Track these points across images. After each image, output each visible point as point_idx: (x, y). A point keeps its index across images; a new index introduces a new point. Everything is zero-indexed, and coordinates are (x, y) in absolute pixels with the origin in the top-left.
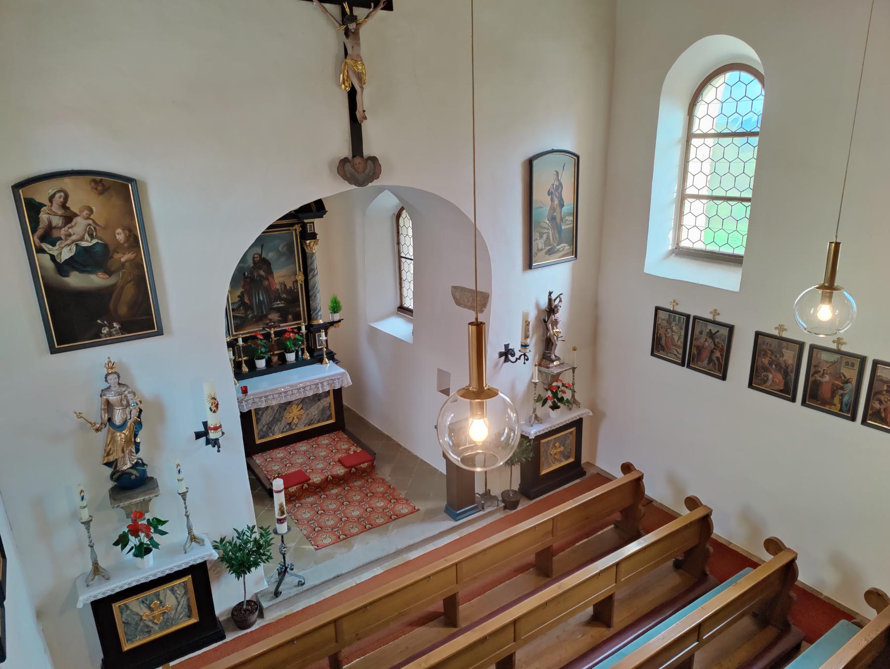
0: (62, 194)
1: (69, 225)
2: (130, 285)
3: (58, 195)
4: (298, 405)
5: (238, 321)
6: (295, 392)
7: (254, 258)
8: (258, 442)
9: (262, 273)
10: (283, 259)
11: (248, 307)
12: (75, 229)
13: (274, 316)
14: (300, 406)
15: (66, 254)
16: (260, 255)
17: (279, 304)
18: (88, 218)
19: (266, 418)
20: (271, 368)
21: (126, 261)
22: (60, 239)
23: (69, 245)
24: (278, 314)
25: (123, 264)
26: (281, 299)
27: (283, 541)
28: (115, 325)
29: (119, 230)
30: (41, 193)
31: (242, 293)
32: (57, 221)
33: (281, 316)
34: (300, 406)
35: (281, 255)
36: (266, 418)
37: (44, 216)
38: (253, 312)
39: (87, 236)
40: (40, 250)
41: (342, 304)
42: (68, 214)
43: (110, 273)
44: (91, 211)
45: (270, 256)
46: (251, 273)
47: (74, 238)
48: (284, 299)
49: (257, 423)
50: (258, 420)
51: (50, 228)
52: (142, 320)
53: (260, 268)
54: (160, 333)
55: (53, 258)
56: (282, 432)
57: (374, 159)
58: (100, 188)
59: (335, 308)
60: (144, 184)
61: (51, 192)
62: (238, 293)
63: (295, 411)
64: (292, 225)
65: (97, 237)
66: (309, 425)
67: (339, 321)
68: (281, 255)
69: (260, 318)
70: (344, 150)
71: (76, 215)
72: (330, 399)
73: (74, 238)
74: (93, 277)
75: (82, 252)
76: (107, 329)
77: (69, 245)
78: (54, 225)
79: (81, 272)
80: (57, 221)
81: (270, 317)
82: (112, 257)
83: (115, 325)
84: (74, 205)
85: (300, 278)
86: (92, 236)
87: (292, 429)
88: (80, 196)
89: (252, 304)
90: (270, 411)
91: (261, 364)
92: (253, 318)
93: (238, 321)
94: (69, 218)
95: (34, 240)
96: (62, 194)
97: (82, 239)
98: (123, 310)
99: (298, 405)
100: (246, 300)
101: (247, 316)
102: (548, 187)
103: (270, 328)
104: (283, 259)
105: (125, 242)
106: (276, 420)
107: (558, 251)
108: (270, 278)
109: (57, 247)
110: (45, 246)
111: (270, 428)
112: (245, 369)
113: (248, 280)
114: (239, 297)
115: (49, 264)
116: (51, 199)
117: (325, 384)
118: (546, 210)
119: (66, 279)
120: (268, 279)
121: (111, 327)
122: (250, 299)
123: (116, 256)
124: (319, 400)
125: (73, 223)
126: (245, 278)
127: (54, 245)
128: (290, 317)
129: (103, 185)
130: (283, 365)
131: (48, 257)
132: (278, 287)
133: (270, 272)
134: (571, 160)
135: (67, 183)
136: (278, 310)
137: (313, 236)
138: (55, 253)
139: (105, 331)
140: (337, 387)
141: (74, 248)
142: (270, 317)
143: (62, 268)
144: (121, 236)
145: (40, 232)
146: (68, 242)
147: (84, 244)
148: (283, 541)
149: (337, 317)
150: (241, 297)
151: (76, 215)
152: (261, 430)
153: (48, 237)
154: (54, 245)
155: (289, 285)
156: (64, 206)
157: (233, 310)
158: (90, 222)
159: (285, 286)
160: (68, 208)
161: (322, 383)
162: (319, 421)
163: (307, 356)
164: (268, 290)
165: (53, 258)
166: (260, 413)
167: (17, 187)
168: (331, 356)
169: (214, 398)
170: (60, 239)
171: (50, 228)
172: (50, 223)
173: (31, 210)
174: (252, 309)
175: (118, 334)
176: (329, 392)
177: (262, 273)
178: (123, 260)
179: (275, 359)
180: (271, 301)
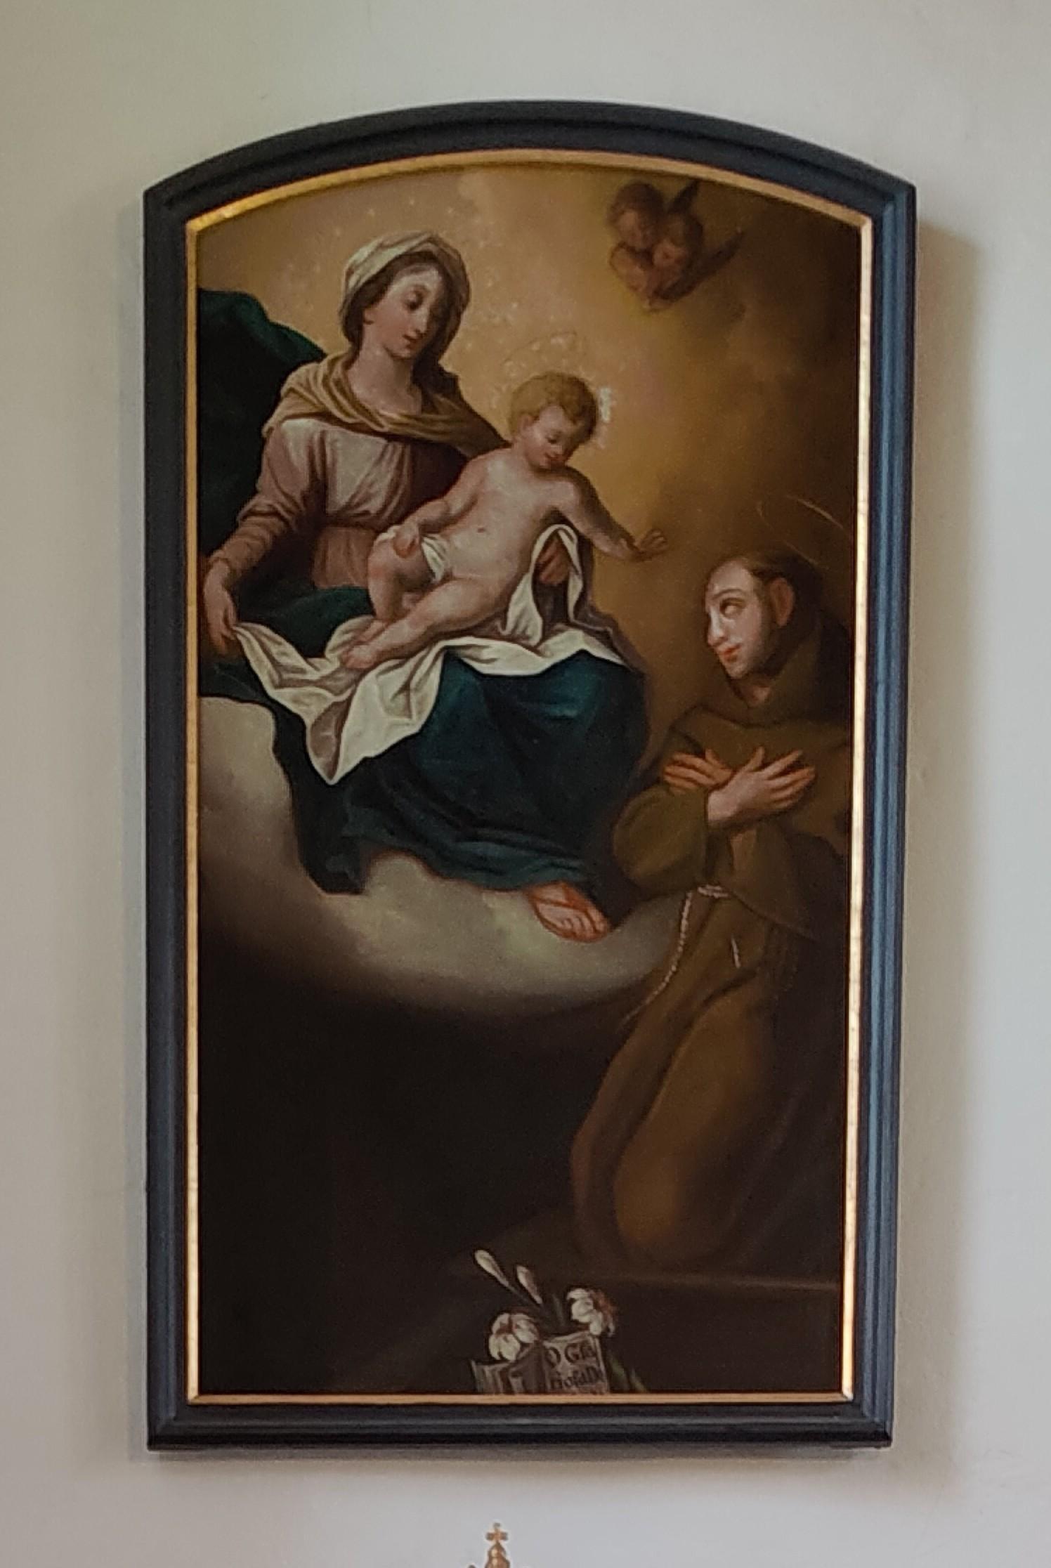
0: (430, 279)
1: (431, 511)
2: (727, 1008)
3: (402, 286)
12: (460, 539)
15: (377, 718)
18: (556, 469)
21: (735, 824)
22: (360, 604)
23: (401, 655)
25: (716, 840)
28: (581, 1305)
29: (737, 579)
30: (305, 275)
32: (363, 470)
37: (291, 430)
39: (523, 602)
40: (231, 678)
42: (439, 427)
43: (616, 896)
44: (584, 412)
47: (443, 603)
51: (316, 516)
55: (289, 729)
58: (669, 251)
61: (368, 258)
65: (585, 617)
71: (486, 439)
73: (443, 603)
75: (481, 713)
76: (525, 1332)
77: (401, 655)
78: (341, 496)
79: (443, 864)
80: (363, 470)
82: (653, 779)
83: (581, 1305)
84: (486, 372)
86: (555, 611)
88: (544, 305)
94: (438, 456)
95: (211, 589)
96: (430, 279)
97: (489, 621)
98: (652, 1199)
105: (765, 667)
109: (329, 664)
110: (266, 651)
115: (260, 780)
116: (354, 322)
119: (338, 903)
121: (552, 1319)
123: (687, 772)
125: (457, 498)
127: (312, 649)
129: (696, 230)
131: (257, 726)
135: (476, 203)
138: (309, 706)
139: (510, 1340)
141: (429, 675)
143: (342, 820)
144: (736, 630)
145: (239, 549)
146: (404, 631)
147: (500, 658)
151: (486, 439)
153: (295, 590)
154: (312, 649)
156: (425, 370)
158: (564, 495)
160: (449, 384)
165: (290, 736)
167: (172, 202)
170: (360, 604)
171: (316, 516)
172: (320, 484)
173: (215, 367)
175: (584, 1380)
178: (720, 806)
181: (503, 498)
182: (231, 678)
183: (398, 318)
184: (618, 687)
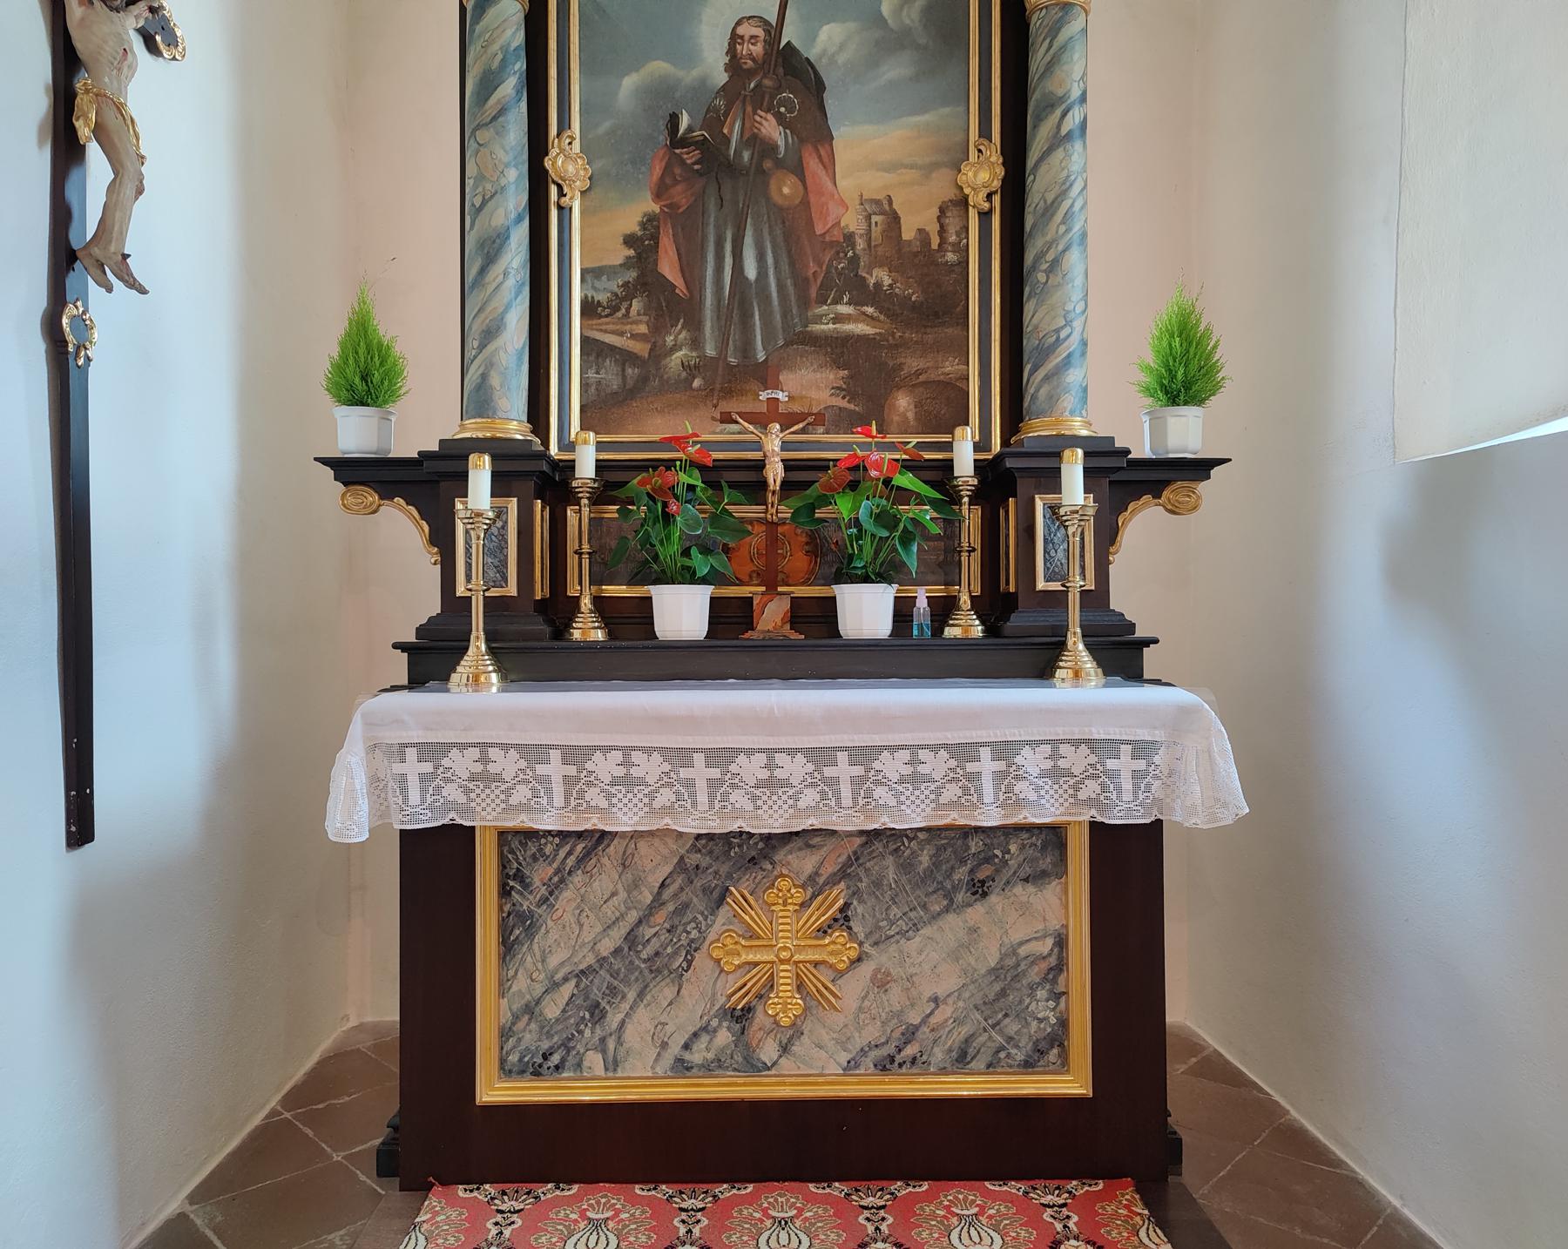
4: (815, 886)
5: (610, 375)
6: (794, 769)
7: (735, 38)
8: (492, 1090)
9: (770, 128)
10: (896, 69)
13: (810, 384)
14: (838, 895)
16: (773, 32)
17: (850, 320)
20: (731, 647)
24: (833, 376)
26: (862, 294)
31: (650, 222)
33: (849, 392)
34: (838, 895)
38: (696, 343)
41: (1233, 357)
45: (826, 41)
46: (714, 120)
48: (874, 296)
49: (507, 947)
50: (517, 930)
53: (761, 100)
56: (682, 1067)
59: (1184, 378)
62: (630, 221)
63: (775, 928)
66: (885, 1066)
67: (1200, 468)
68: (889, 41)
69: (732, 379)
72: (1064, 908)
85: (983, 175)
87: (753, 1066)
90: (604, 880)
91: (682, 612)
92: (691, 370)
93: (610, 375)
99: (815, 886)
100: (668, 267)
101: (659, 354)
103: (761, 421)
104: (896, 69)
106: (646, 960)
108: (812, 164)
111: (597, 1013)
112: (588, 629)
113: (691, 156)
114: (629, 241)
117: (1032, 761)
120: (799, 171)
122: (690, 265)
124: (980, 890)
126: (677, 141)
128: (903, 403)
130: (816, 647)
132: (852, 221)
133: (814, 130)
136: (839, 350)
140: (1125, 811)
149: (1186, 433)
150: (643, 245)
152: (531, 1010)
155: (917, 220)
157: (589, 308)
159: (894, 220)
161: (1005, 750)
162: (962, 1059)
163: (967, 626)
164: (793, 229)
166: (540, 874)
168: (1122, 653)
174: (694, 324)
176: (1055, 835)
177: (770, 128)
179: (772, 616)
180: (805, 294)
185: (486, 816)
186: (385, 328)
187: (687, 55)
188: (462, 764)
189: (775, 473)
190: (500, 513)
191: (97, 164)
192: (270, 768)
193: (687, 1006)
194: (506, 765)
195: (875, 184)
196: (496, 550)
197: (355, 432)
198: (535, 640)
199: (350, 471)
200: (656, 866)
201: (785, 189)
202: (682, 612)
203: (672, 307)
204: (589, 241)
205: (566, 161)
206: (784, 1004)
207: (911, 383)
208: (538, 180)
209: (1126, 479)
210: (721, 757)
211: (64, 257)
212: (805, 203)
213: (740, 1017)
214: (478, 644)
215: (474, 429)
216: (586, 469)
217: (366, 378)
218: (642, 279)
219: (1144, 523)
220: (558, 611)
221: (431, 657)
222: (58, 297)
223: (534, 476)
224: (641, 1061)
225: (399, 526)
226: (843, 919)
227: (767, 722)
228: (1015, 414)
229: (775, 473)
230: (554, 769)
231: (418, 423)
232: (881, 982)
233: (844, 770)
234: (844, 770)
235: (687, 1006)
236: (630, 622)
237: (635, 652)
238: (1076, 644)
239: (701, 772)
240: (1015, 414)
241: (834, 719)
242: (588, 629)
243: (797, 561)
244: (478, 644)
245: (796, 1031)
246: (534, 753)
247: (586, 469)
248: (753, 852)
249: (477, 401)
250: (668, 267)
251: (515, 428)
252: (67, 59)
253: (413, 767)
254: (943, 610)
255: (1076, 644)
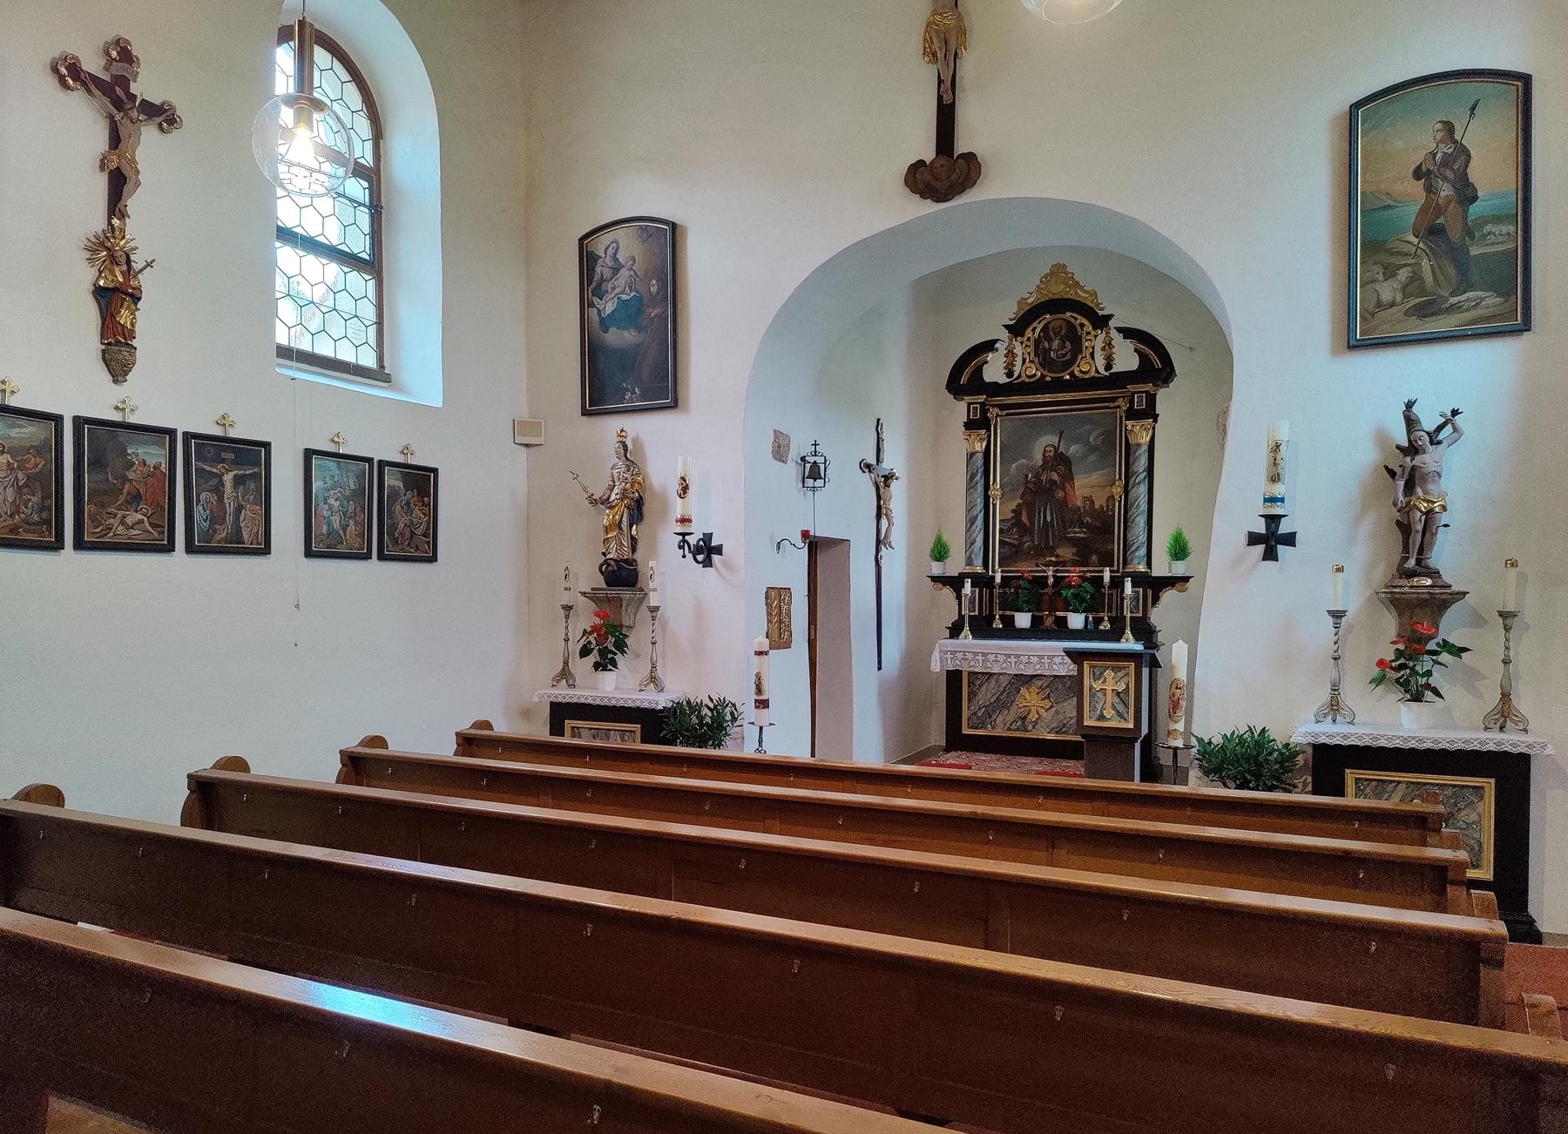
8: (966, 731)
11: (1024, 530)
13: (1066, 552)
14: (1047, 691)
15: (609, 307)
16: (1056, 449)
17: (1078, 533)
19: (986, 695)
20: (1037, 631)
26: (1082, 525)
27: (760, 742)
30: (601, 245)
32: (607, 273)
33: (1077, 554)
34: (1047, 691)
35: (1093, 449)
36: (986, 695)
37: (598, 269)
41: (1192, 545)
43: (639, 329)
45: (1073, 450)
46: (1037, 476)
48: (1087, 526)
51: (602, 280)
52: (662, 388)
54: (674, 405)
57: (970, 158)
59: (1179, 551)
60: (684, 228)
62: (1013, 505)
63: (1030, 698)
64: (1114, 399)
67: (1186, 579)
70: (929, 154)
74: (626, 334)
75: (623, 304)
80: (607, 273)
81: (1059, 551)
84: (621, 257)
85: (1118, 490)
87: (1026, 730)
88: (627, 245)
89: (1032, 524)
91: (1023, 620)
94: (616, 270)
100: (1024, 519)
101: (1020, 545)
102: (1418, 158)
104: (1092, 458)
107: (1453, 309)
110: (596, 300)
112: (998, 624)
118: (1410, 213)
122: (1031, 517)
132: (1079, 503)
133: (1068, 477)
134: (1512, 90)
135: (620, 234)
136: (1075, 542)
137: (1150, 413)
142: (1059, 551)
143: (605, 324)
144: (654, 289)
147: (624, 297)
148: (760, 742)
149: (1179, 569)
150: (1017, 512)
159: (1092, 502)
164: (1063, 505)
169: (683, 479)
171: (602, 280)
173: (587, 260)
177: (1055, 477)
179: (1049, 622)
181: (624, 273)
182: (592, 305)
183: (610, 252)
184: (641, 299)
185: (965, 668)
186: (945, 539)
187: (1029, 457)
188: (960, 656)
189: (1051, 581)
190: (973, 592)
191: (884, 522)
192: (915, 657)
193: (1012, 714)
194: (970, 656)
195: (1087, 492)
196: (972, 602)
197: (937, 569)
198: (982, 628)
199: (935, 579)
200: (1004, 681)
201: (1060, 494)
202: (1023, 620)
203: (1024, 530)
204: (1001, 511)
205: (995, 491)
206: (1033, 717)
207: (1097, 552)
208: (987, 498)
209: (1155, 586)
210: (1018, 656)
211: (878, 542)
212: (1065, 498)
213: (1024, 719)
214: (967, 628)
215: (968, 570)
216: (998, 580)
217: (940, 553)
218: (1015, 524)
219: (1168, 596)
220: (991, 618)
221: (955, 631)
222: (878, 551)
223: (982, 581)
224: (999, 728)
225: (948, 593)
226: (1048, 697)
227: (1027, 649)
228: (1125, 563)
229: (1051, 581)
230: (980, 658)
231: (955, 565)
232: (1057, 712)
233: (1046, 660)
234: (1046, 660)
235: (1012, 714)
236: (1009, 621)
237: (1010, 631)
238: (1128, 631)
239: (1013, 659)
240: (1125, 563)
241: (1043, 649)
242: (998, 624)
243: (1061, 605)
244: (967, 628)
245: (1036, 723)
246: (976, 654)
247: (998, 580)
248: (1027, 680)
249: (969, 562)
250: (1024, 519)
251: (979, 570)
252: (879, 498)
253: (949, 656)
254: (1098, 621)
255: (1128, 631)
